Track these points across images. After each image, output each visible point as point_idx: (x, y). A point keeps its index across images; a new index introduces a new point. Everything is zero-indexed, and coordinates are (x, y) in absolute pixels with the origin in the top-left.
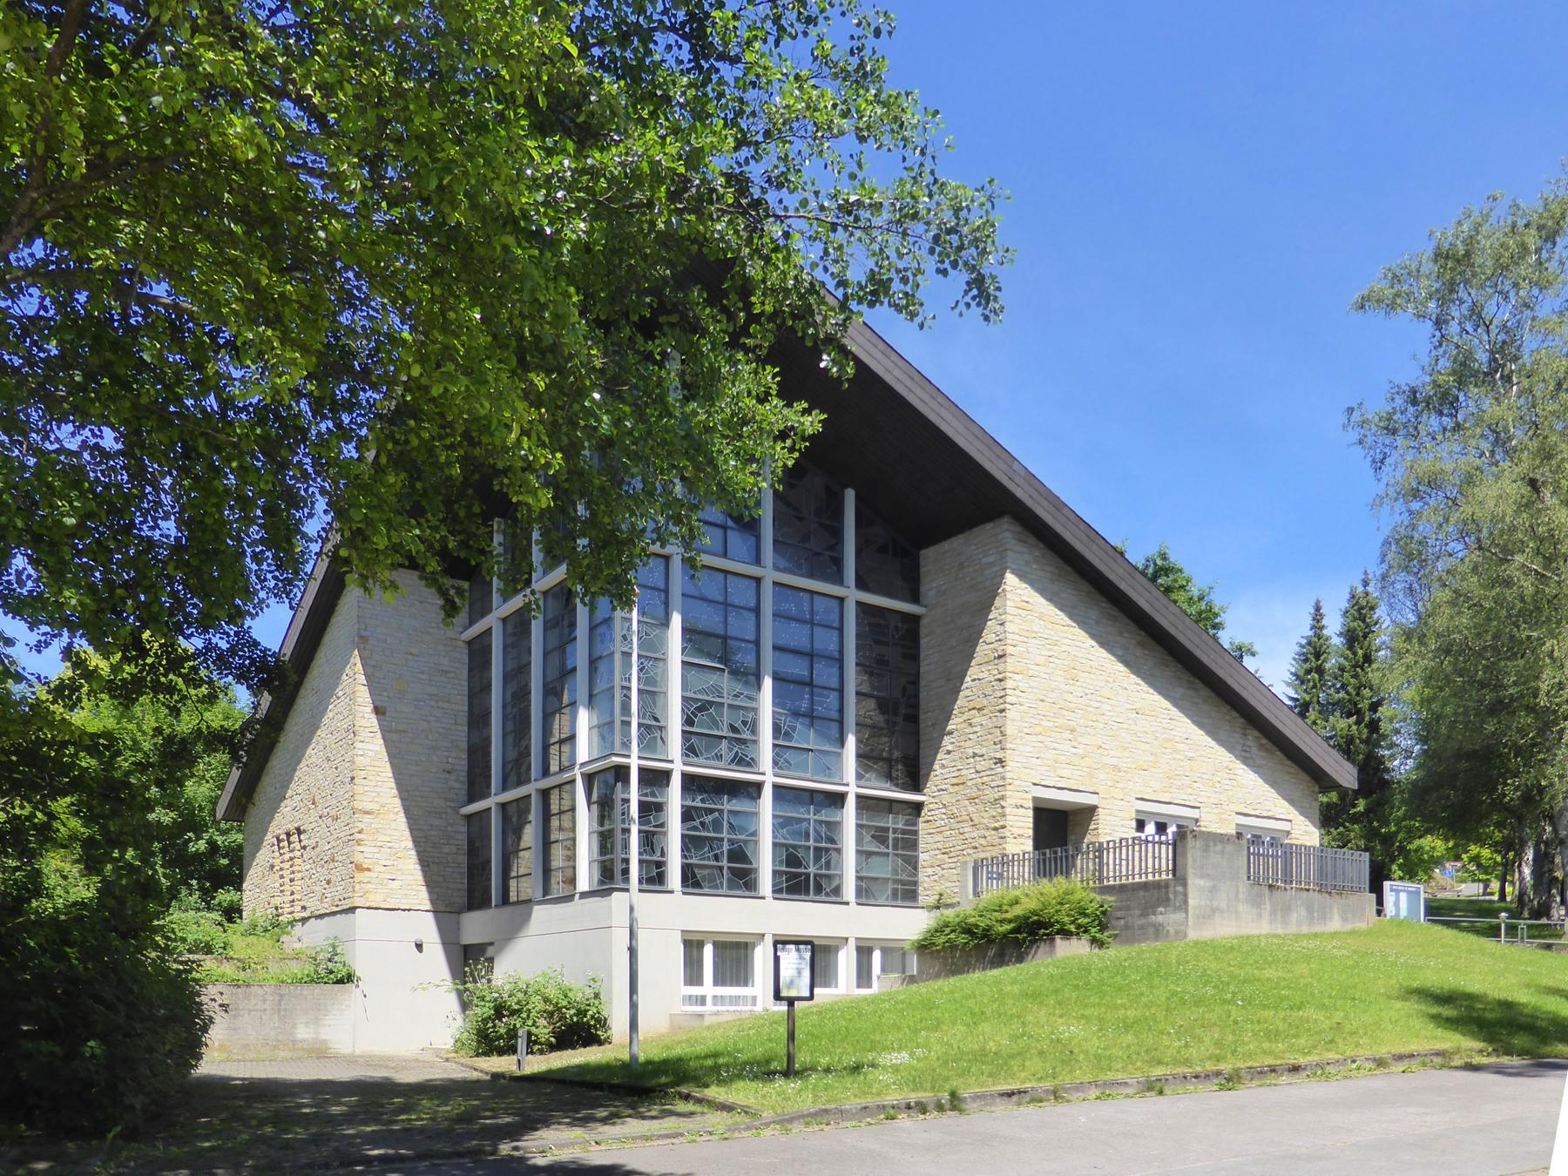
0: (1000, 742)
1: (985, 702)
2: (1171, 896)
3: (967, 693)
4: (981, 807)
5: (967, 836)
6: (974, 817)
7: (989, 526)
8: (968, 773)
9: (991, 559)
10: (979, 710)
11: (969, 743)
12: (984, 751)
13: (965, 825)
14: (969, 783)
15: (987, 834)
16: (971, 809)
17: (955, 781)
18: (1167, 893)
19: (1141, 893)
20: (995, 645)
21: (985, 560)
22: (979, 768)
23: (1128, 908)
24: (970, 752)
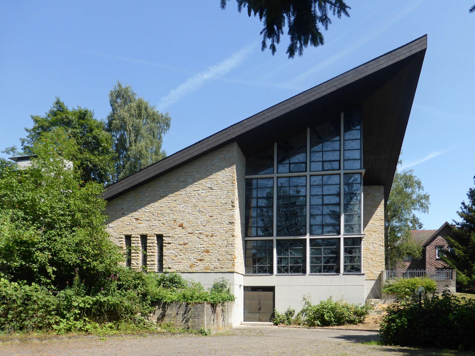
0: (382, 241)
1: (376, 230)
2: (451, 284)
3: (370, 227)
4: (375, 256)
5: (370, 263)
6: (373, 258)
7: (378, 186)
8: (371, 247)
9: (379, 195)
10: (374, 232)
11: (370, 239)
12: (376, 242)
13: (370, 260)
14: (371, 250)
15: (378, 263)
16: (371, 256)
17: (366, 248)
18: (450, 283)
19: (443, 282)
20: (380, 217)
21: (376, 195)
22: (374, 246)
23: (439, 285)
24: (371, 242)
